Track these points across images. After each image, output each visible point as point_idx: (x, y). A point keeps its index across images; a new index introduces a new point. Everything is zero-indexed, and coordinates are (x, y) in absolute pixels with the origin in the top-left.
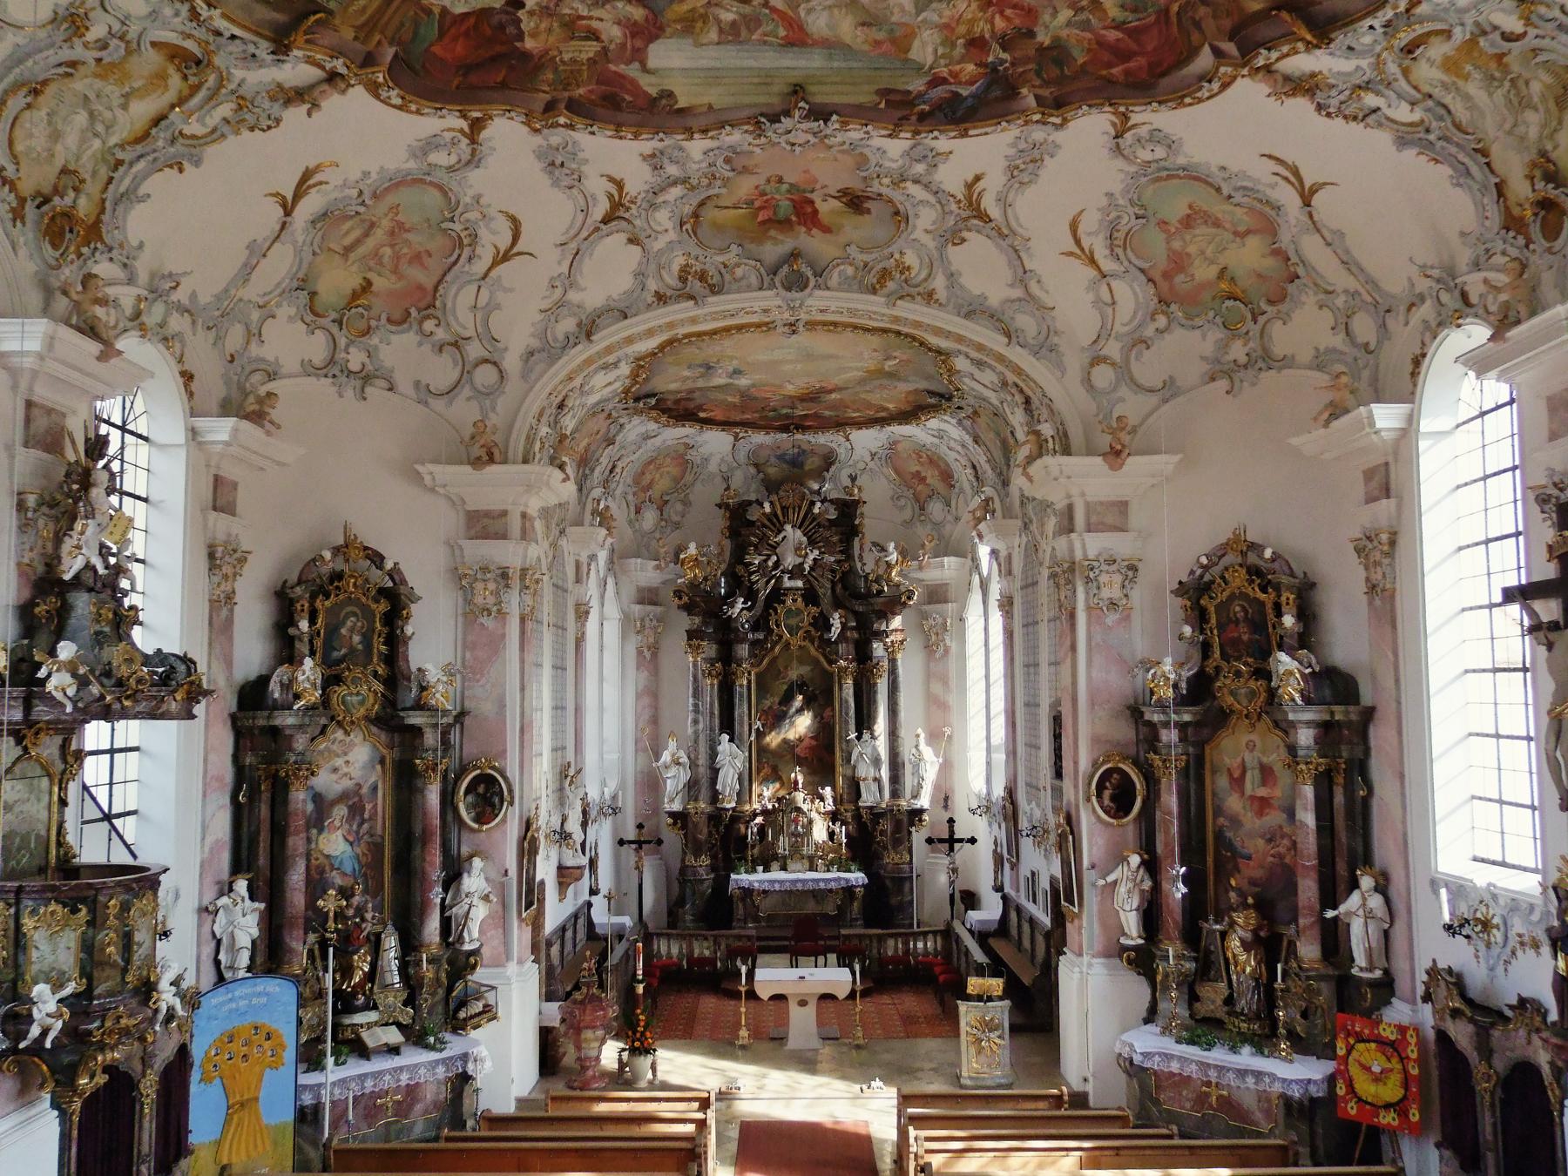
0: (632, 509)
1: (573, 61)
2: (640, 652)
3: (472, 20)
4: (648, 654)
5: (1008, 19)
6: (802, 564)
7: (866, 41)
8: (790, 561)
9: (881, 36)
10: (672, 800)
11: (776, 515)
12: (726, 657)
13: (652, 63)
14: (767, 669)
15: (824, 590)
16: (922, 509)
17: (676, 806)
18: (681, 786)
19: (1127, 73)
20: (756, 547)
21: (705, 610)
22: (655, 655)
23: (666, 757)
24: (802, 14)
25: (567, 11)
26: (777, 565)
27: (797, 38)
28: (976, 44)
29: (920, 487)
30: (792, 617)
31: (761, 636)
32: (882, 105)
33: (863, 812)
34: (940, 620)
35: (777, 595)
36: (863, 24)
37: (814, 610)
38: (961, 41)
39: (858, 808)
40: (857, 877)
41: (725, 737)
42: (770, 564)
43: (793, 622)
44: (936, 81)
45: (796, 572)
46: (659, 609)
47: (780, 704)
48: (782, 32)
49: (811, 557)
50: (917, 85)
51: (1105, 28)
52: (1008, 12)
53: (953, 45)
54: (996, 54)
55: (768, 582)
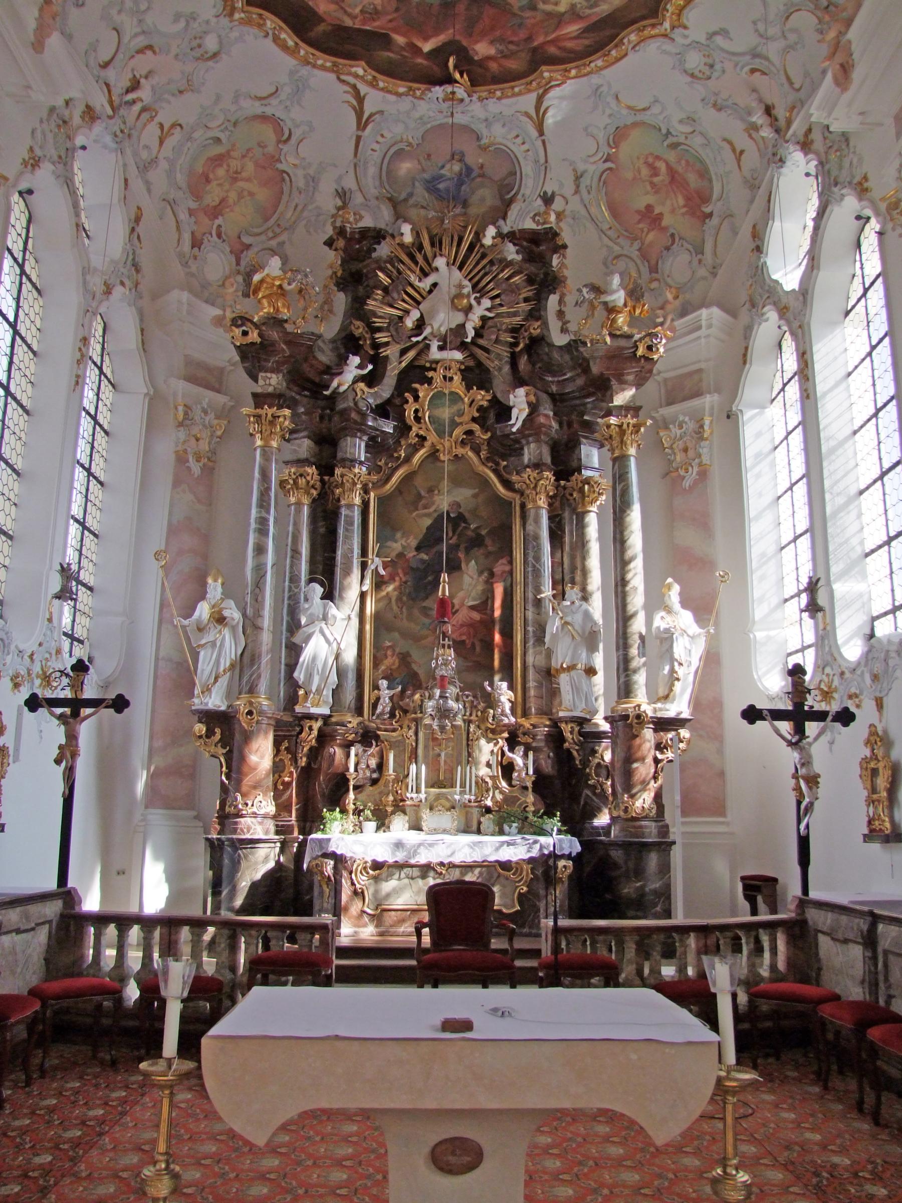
0: (187, 237)
2: (181, 459)
4: (196, 468)
6: (462, 326)
8: (443, 320)
10: (207, 690)
11: (420, 248)
12: (327, 458)
14: (399, 490)
15: (498, 365)
16: (654, 269)
17: (216, 701)
18: (225, 663)
20: (386, 290)
21: (294, 375)
22: (209, 471)
23: (203, 610)
26: (420, 324)
29: (651, 237)
30: (444, 407)
31: (388, 427)
33: (566, 729)
34: (691, 426)
35: (416, 373)
37: (482, 397)
39: (555, 724)
40: (555, 840)
41: (318, 590)
42: (409, 323)
43: (445, 413)
45: (454, 338)
46: (221, 399)
47: (418, 549)
49: (479, 311)
55: (403, 352)
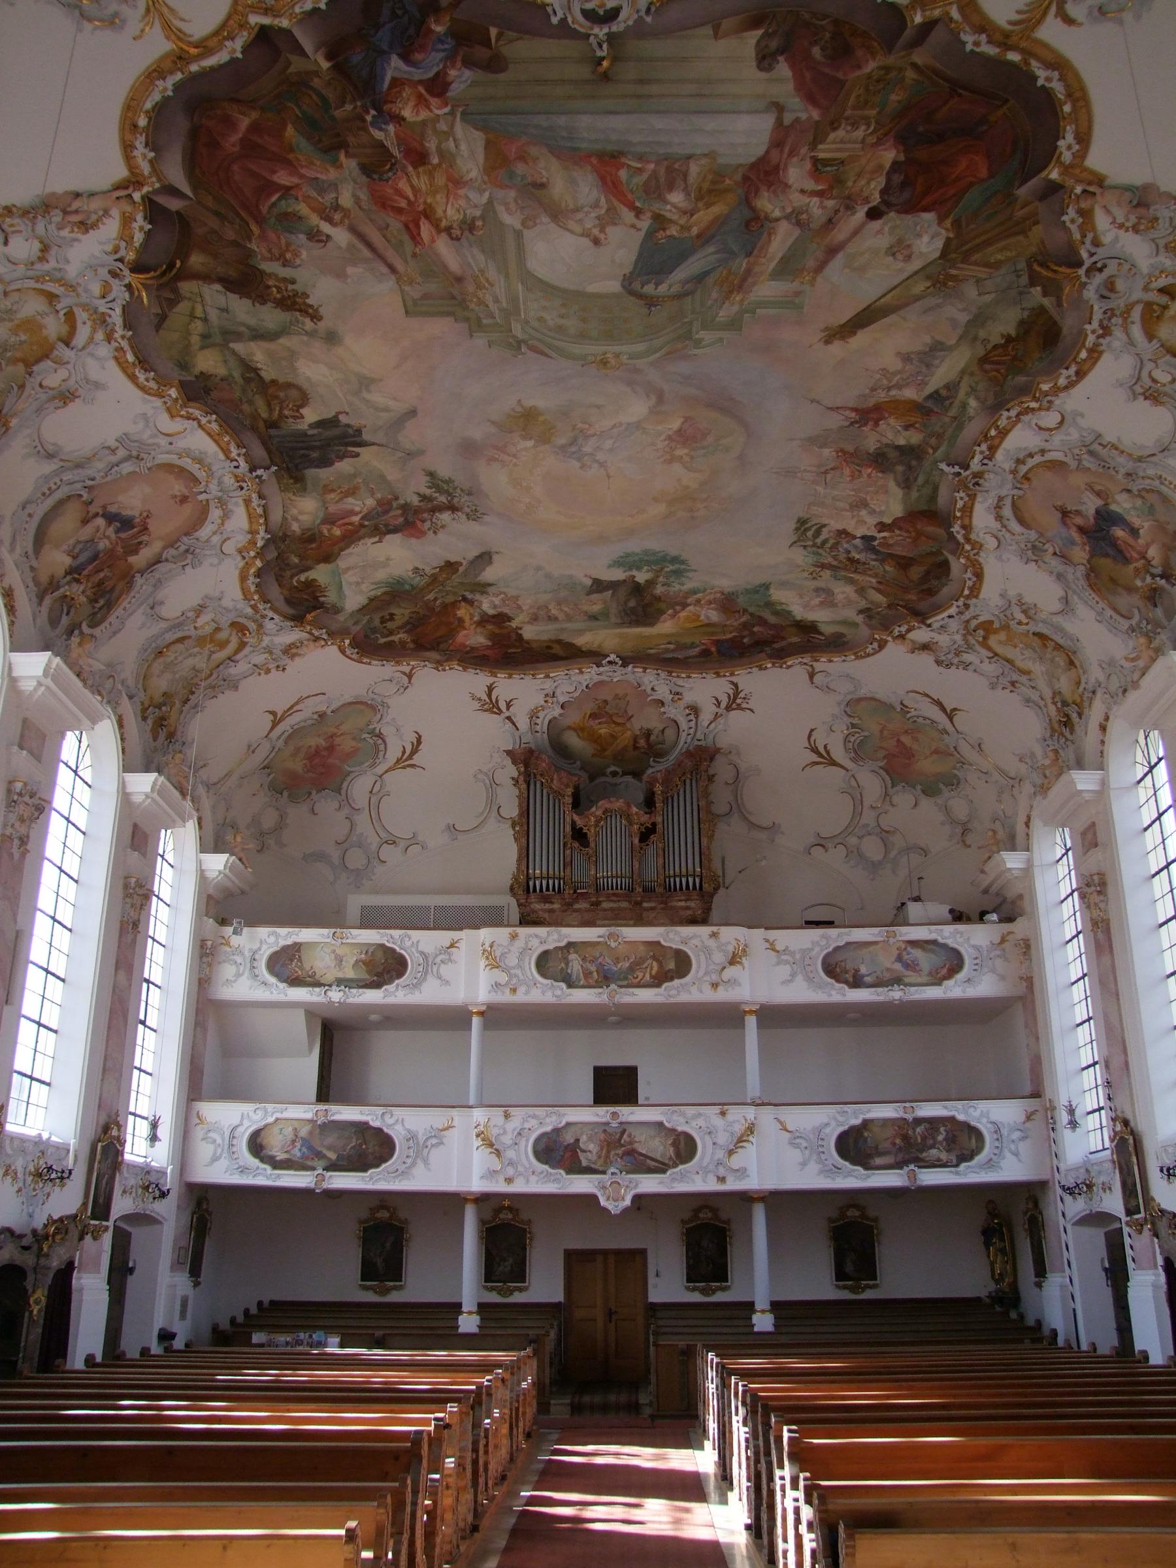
1: (855, 125)
3: (924, 203)
5: (400, 193)
7: (536, 159)
9: (520, 169)
13: (765, 124)
19: (229, 123)
24: (603, 200)
25: (830, 203)
27: (606, 162)
28: (419, 158)
32: (493, 32)
36: (542, 186)
38: (435, 161)
44: (438, 86)
48: (623, 174)
50: (461, 79)
51: (297, 186)
52: (403, 204)
53: (441, 153)
54: (387, 135)
